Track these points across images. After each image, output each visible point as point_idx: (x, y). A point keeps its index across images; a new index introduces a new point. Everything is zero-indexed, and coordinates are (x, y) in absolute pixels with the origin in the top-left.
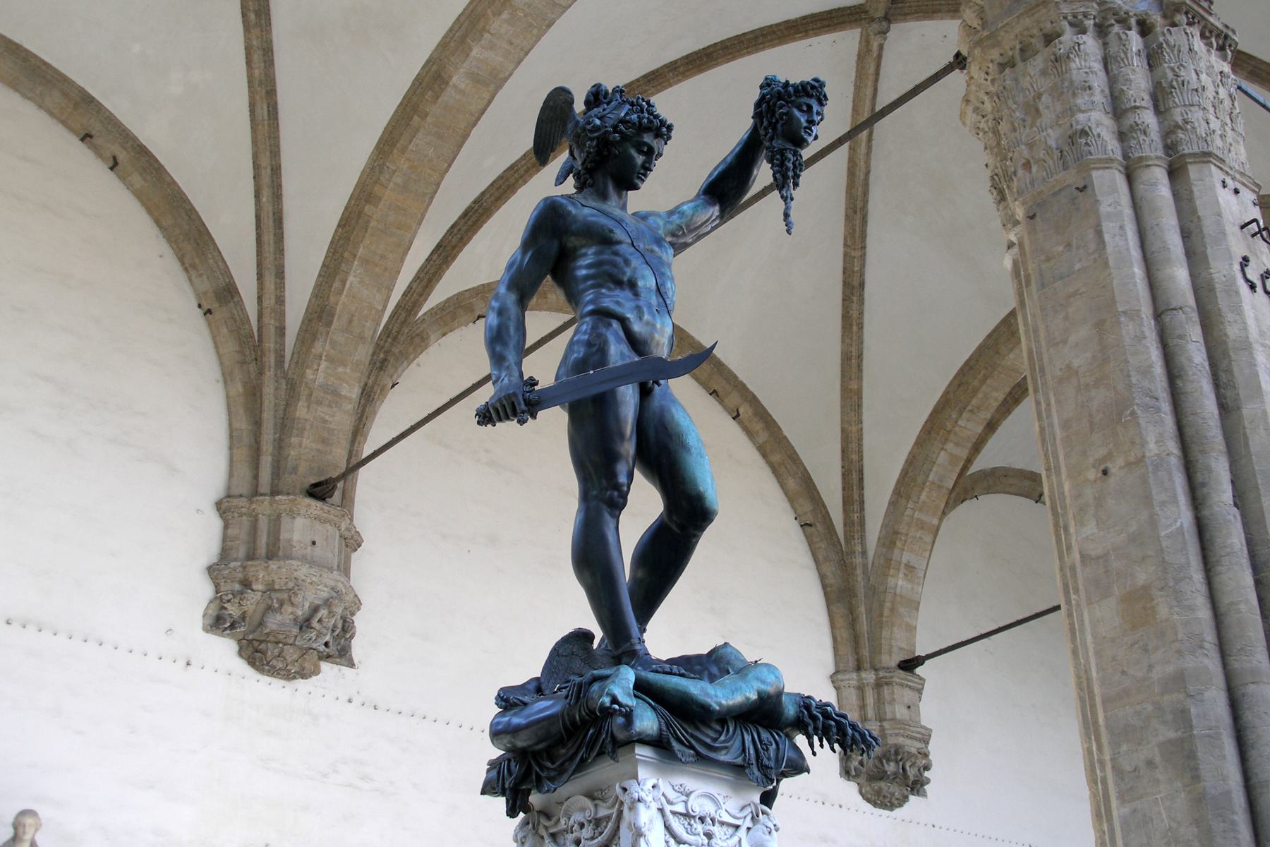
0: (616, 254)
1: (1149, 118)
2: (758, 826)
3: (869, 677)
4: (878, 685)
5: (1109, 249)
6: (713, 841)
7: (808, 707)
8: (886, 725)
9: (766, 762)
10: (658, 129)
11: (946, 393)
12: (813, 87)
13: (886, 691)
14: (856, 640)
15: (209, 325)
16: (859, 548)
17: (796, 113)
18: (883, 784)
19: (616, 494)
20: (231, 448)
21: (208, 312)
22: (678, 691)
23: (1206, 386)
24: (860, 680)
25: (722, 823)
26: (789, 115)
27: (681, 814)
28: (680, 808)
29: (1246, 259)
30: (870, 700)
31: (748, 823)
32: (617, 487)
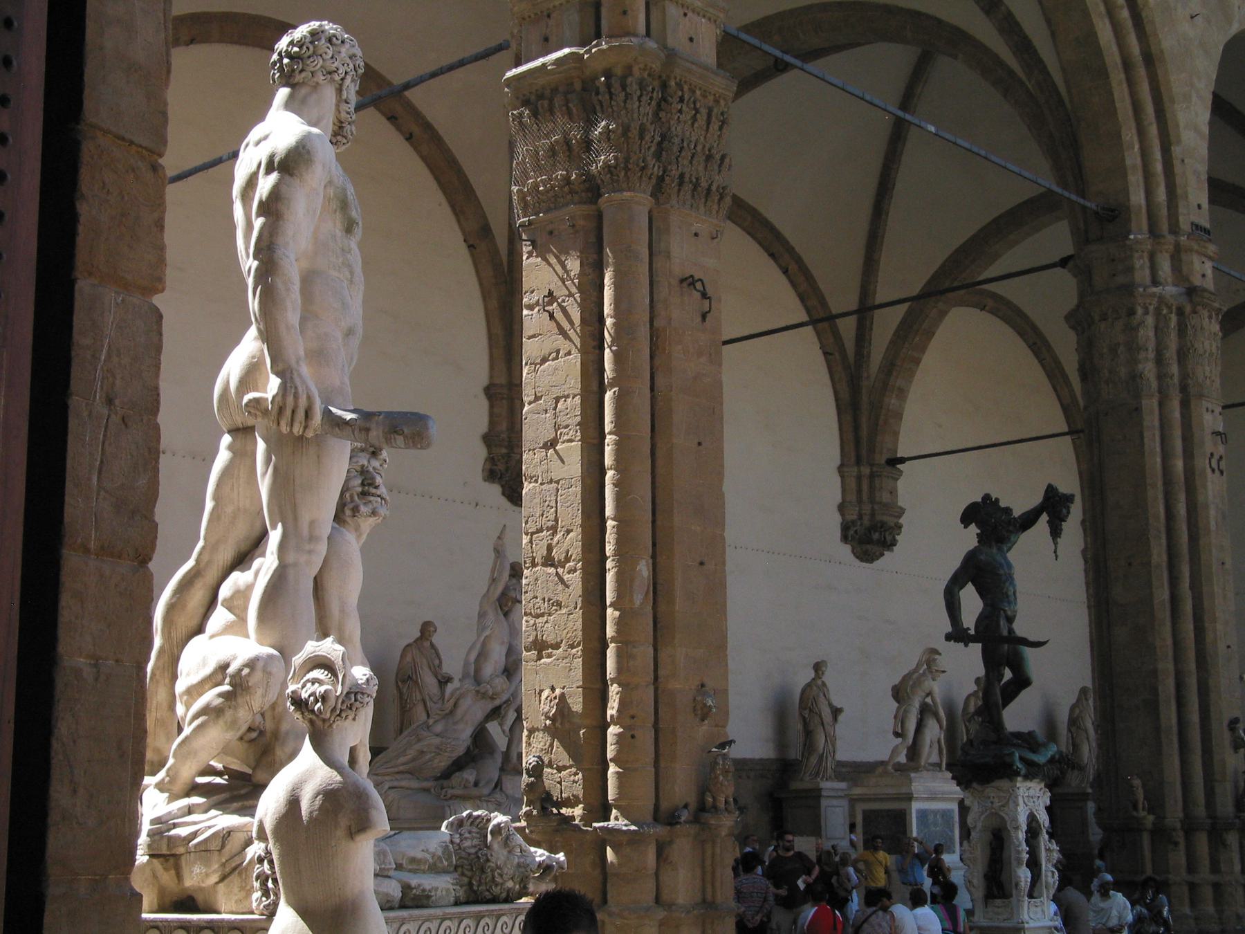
1: (1175, 369)
3: (866, 470)
4: (872, 476)
5: (1146, 446)
8: (876, 507)
11: (943, 266)
13: (877, 481)
14: (857, 442)
15: (472, 255)
16: (865, 375)
18: (869, 547)
20: (491, 347)
21: (471, 247)
23: (1184, 527)
24: (859, 471)
29: (1212, 455)
30: (865, 487)
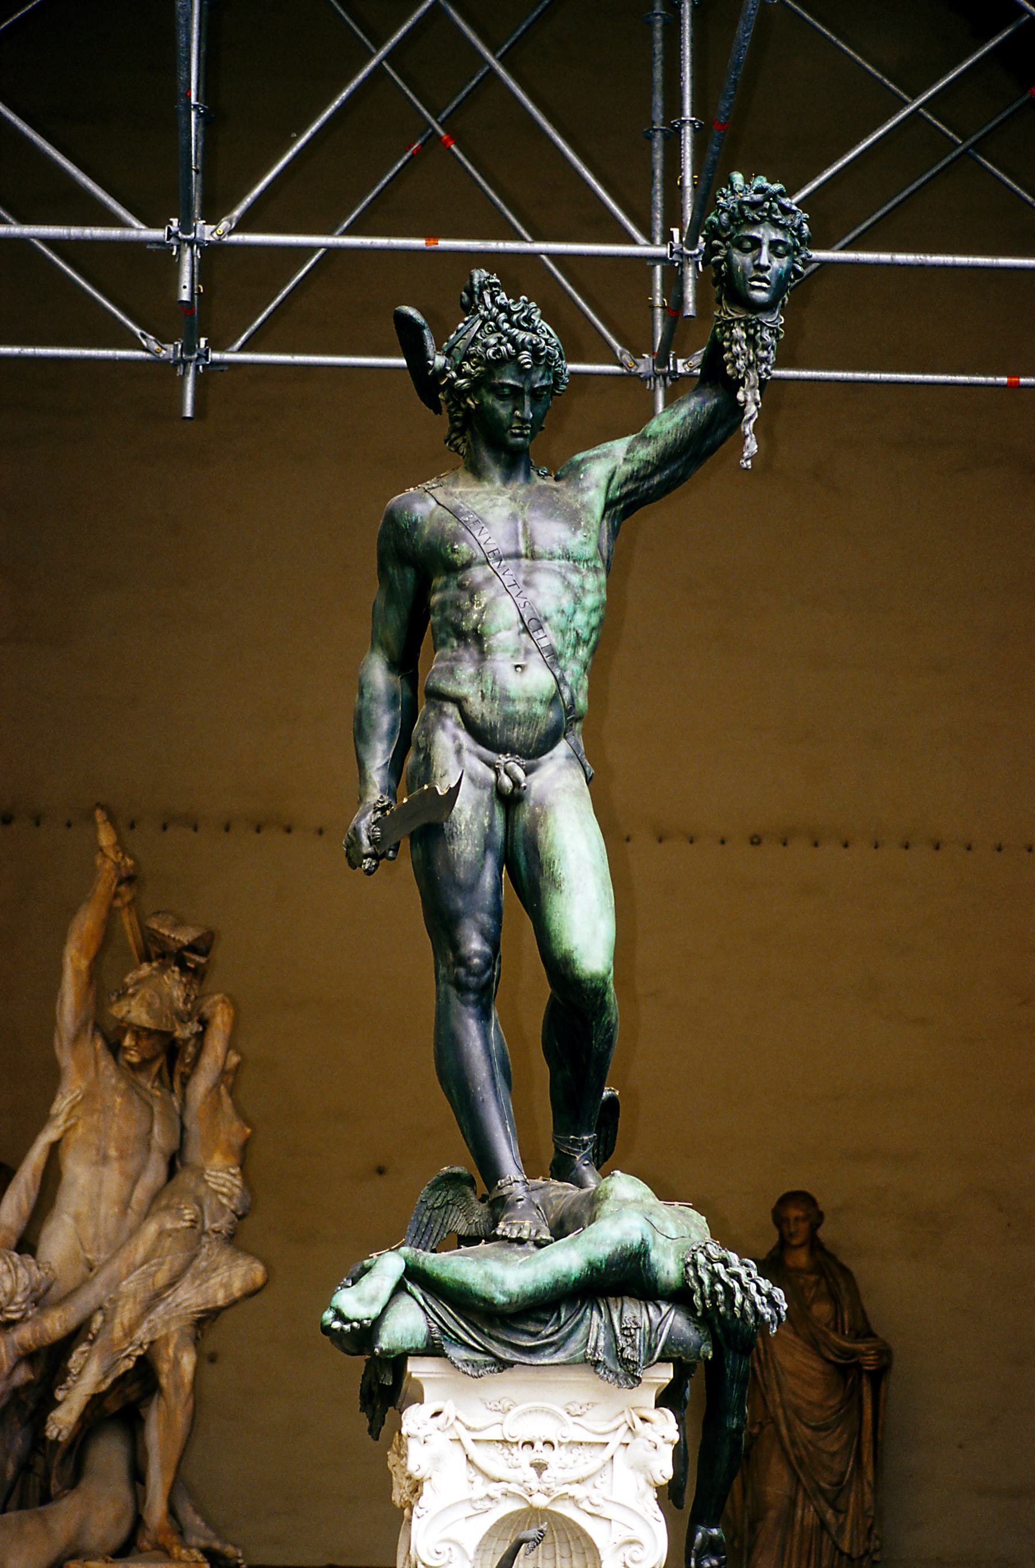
0: (461, 586)
2: (638, 1440)
6: (545, 1474)
7: (694, 1264)
9: (628, 1353)
10: (513, 358)
12: (754, 205)
17: (738, 257)
19: (462, 971)
22: (455, 1281)
25: (570, 1443)
26: (728, 258)
27: (498, 1441)
28: (495, 1434)
31: (622, 1435)
32: (462, 961)
